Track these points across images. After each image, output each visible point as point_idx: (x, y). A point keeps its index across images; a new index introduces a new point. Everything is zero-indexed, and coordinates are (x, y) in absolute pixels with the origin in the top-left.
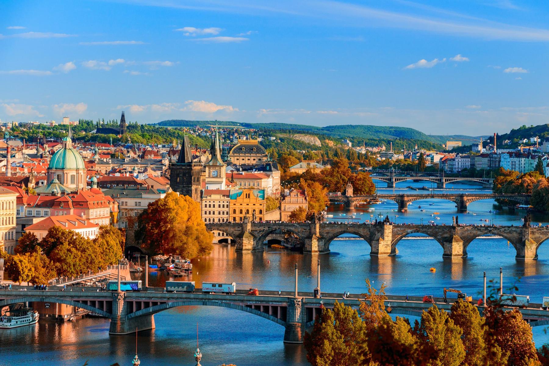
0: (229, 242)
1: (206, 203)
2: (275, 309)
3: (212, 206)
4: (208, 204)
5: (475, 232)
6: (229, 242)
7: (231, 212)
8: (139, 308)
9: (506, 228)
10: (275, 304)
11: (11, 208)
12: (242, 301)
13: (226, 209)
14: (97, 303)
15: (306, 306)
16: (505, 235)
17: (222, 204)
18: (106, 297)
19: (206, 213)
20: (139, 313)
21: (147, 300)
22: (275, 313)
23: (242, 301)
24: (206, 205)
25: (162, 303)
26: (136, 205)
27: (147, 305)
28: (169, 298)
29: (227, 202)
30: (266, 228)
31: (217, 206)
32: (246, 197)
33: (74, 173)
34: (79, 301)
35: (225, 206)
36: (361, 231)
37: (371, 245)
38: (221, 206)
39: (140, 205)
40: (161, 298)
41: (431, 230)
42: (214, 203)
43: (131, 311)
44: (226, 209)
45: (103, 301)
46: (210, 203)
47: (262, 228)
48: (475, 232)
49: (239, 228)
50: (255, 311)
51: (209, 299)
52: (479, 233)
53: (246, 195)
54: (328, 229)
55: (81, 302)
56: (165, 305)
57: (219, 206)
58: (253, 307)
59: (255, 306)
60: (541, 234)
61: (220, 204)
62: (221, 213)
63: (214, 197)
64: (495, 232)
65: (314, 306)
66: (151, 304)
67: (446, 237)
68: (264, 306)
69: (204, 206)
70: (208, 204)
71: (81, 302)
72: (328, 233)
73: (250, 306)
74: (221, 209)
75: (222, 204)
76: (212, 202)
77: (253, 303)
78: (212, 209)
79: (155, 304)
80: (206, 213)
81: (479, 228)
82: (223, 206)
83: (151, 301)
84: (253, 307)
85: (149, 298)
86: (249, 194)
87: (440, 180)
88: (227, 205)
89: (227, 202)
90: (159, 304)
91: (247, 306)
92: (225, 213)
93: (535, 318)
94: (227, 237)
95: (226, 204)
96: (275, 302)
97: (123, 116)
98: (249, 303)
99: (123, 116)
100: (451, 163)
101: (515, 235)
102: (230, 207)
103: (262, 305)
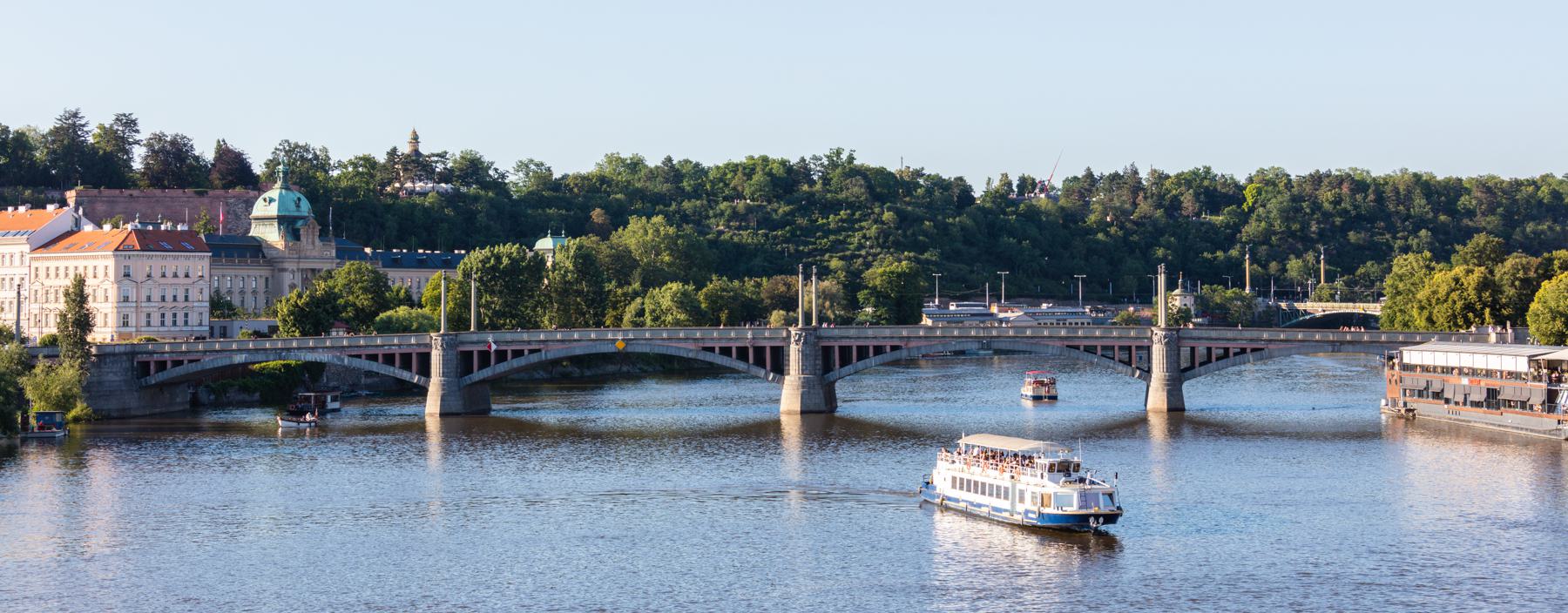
2: (759, 351)
20: (487, 373)
25: (531, 352)
34: (359, 356)
43: (472, 372)
55: (364, 357)
58: (717, 350)
59: (720, 348)
71: (364, 357)
79: (518, 354)
83: (509, 348)
84: (717, 350)
90: (526, 352)
103: (734, 345)
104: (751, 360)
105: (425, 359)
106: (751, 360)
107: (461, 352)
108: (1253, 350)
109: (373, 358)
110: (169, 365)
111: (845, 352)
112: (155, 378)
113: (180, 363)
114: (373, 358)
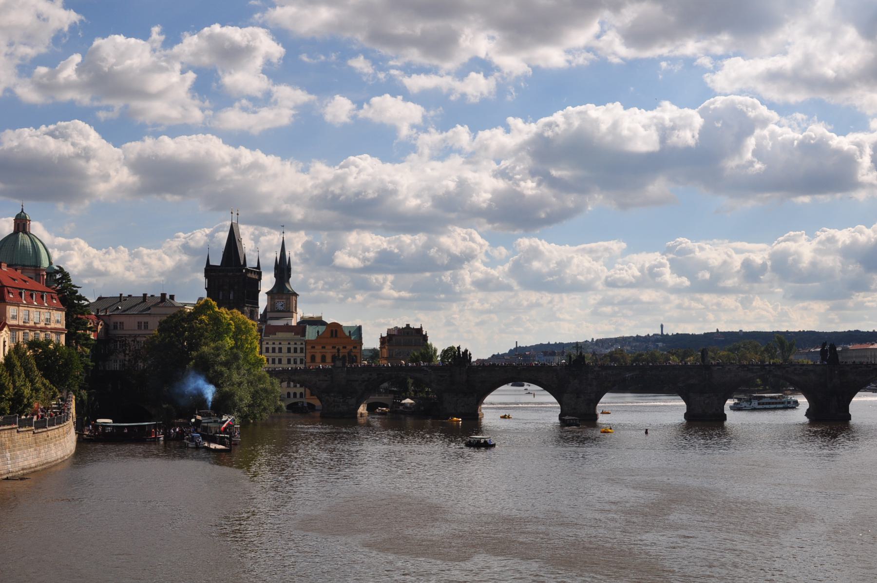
1: (267, 346)
3: (277, 351)
4: (270, 346)
7: (308, 359)
13: (299, 355)
17: (292, 347)
26: (139, 327)
29: (302, 344)
31: (285, 350)
32: (332, 336)
35: (299, 351)
37: (560, 402)
38: (292, 351)
39: (146, 327)
42: (280, 346)
44: (299, 355)
46: (274, 346)
49: (326, 376)
53: (332, 331)
57: (289, 350)
61: (289, 346)
63: (280, 335)
70: (270, 346)
74: (292, 354)
75: (292, 347)
76: (277, 343)
81: (750, 367)
82: (295, 350)
86: (336, 331)
88: (302, 349)
89: (302, 344)
95: (299, 347)
102: (307, 351)
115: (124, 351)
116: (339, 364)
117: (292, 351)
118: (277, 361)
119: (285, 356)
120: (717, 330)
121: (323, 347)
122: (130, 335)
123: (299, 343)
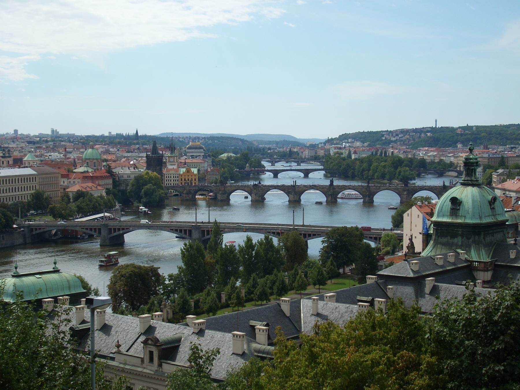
0: (179, 195)
2: (185, 231)
3: (170, 177)
5: (305, 188)
6: (179, 195)
7: (180, 180)
8: (115, 232)
9: (321, 187)
10: (185, 228)
11: (48, 180)
12: (168, 227)
13: (177, 179)
14: (93, 229)
15: (201, 229)
16: (320, 190)
18: (97, 226)
19: (167, 181)
20: (115, 234)
21: (119, 227)
22: (185, 233)
23: (168, 227)
24: (167, 177)
25: (126, 229)
26: (128, 177)
27: (119, 230)
28: (130, 226)
30: (197, 188)
31: (172, 177)
33: (95, 161)
36: (246, 189)
38: (175, 177)
39: (130, 177)
40: (126, 226)
41: (282, 188)
43: (111, 233)
44: (177, 179)
45: (96, 229)
47: (194, 188)
48: (305, 188)
50: (175, 232)
51: (151, 226)
52: (307, 189)
54: (229, 188)
56: (128, 229)
57: (174, 177)
58: (174, 230)
60: (339, 189)
62: (175, 181)
64: (315, 188)
65: (205, 229)
66: (121, 229)
67: (290, 192)
68: (179, 230)
69: (165, 177)
72: (229, 190)
73: (173, 230)
74: (175, 178)
77: (174, 228)
78: (170, 178)
79: (123, 229)
80: (167, 181)
82: (176, 177)
84: (174, 230)
85: (120, 226)
87: (298, 162)
88: (178, 177)
91: (171, 229)
92: (177, 181)
93: (320, 233)
94: (178, 193)
96: (185, 227)
97: (137, 131)
98: (171, 228)
99: (137, 131)
100: (305, 153)
101: (326, 190)
103: (179, 229)
104: (183, 233)
105: (100, 230)
106: (183, 233)
107: (109, 228)
108: (318, 235)
109: (87, 229)
110: (38, 229)
111: (208, 231)
112: (34, 233)
113: (40, 229)
114: (87, 229)
115: (124, 184)
116: (186, 184)
117: (175, 177)
118: (170, 181)
119: (172, 179)
120: (467, 125)
121: (185, 176)
122: (125, 180)
123: (177, 175)
